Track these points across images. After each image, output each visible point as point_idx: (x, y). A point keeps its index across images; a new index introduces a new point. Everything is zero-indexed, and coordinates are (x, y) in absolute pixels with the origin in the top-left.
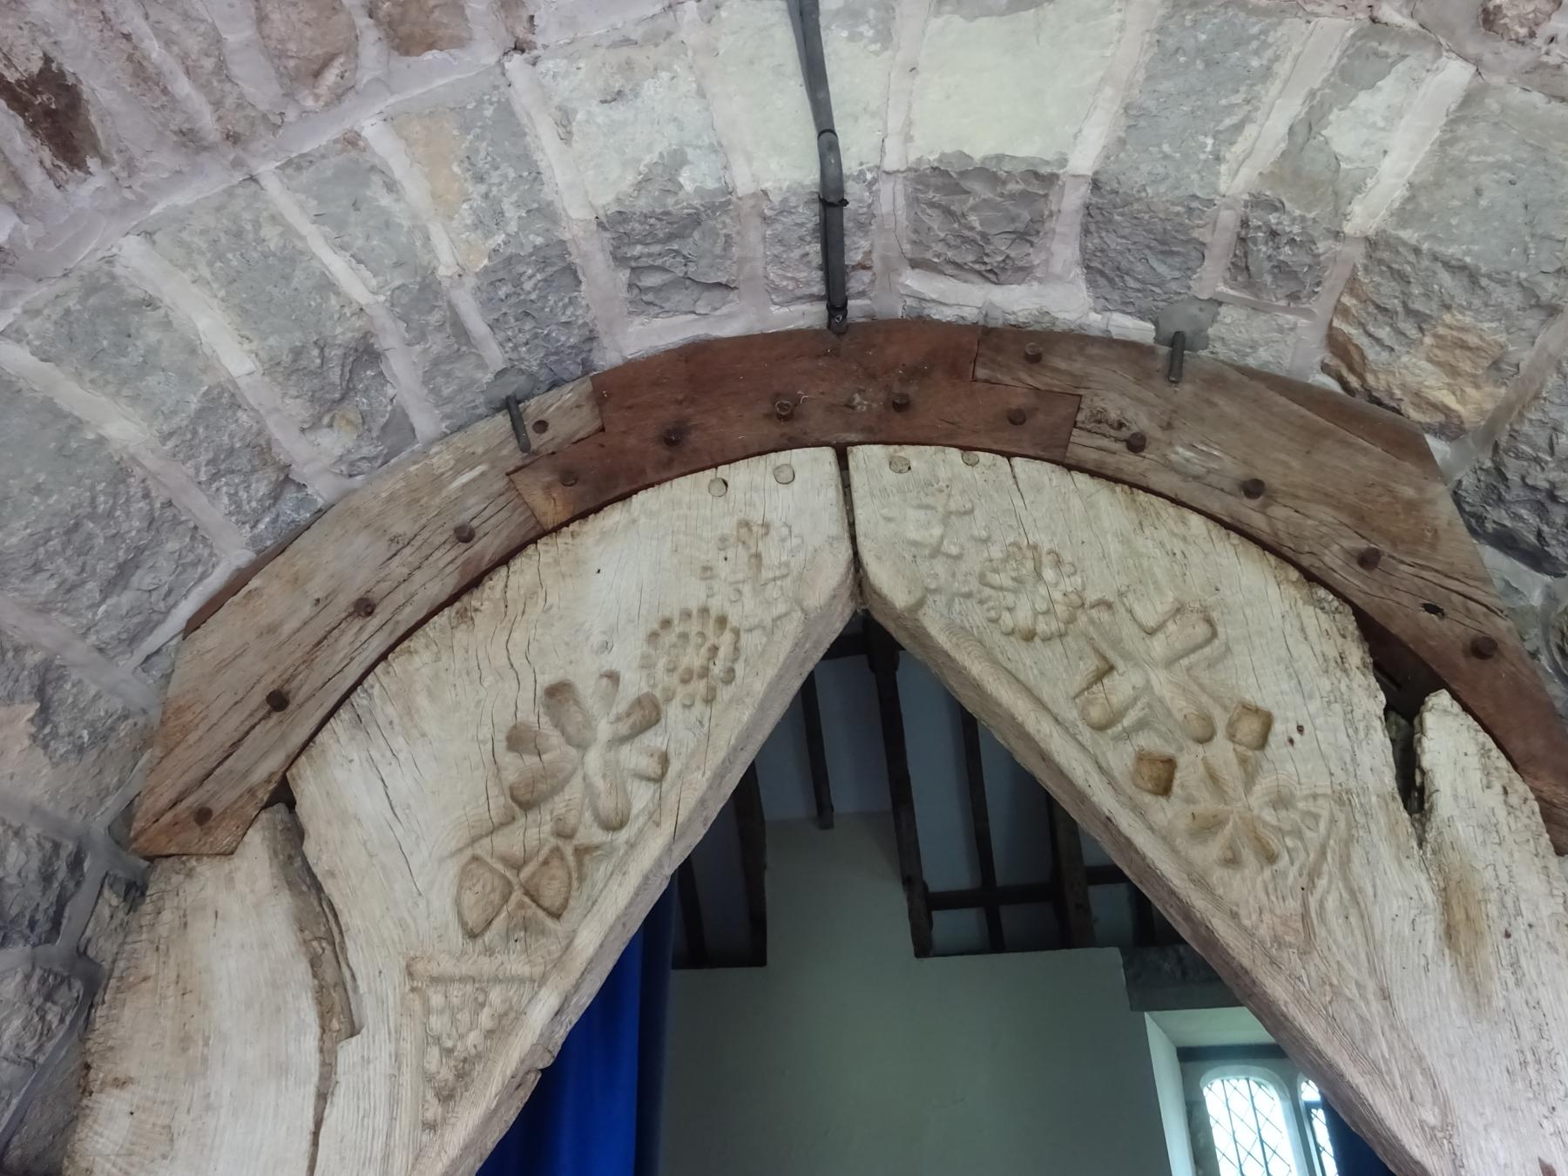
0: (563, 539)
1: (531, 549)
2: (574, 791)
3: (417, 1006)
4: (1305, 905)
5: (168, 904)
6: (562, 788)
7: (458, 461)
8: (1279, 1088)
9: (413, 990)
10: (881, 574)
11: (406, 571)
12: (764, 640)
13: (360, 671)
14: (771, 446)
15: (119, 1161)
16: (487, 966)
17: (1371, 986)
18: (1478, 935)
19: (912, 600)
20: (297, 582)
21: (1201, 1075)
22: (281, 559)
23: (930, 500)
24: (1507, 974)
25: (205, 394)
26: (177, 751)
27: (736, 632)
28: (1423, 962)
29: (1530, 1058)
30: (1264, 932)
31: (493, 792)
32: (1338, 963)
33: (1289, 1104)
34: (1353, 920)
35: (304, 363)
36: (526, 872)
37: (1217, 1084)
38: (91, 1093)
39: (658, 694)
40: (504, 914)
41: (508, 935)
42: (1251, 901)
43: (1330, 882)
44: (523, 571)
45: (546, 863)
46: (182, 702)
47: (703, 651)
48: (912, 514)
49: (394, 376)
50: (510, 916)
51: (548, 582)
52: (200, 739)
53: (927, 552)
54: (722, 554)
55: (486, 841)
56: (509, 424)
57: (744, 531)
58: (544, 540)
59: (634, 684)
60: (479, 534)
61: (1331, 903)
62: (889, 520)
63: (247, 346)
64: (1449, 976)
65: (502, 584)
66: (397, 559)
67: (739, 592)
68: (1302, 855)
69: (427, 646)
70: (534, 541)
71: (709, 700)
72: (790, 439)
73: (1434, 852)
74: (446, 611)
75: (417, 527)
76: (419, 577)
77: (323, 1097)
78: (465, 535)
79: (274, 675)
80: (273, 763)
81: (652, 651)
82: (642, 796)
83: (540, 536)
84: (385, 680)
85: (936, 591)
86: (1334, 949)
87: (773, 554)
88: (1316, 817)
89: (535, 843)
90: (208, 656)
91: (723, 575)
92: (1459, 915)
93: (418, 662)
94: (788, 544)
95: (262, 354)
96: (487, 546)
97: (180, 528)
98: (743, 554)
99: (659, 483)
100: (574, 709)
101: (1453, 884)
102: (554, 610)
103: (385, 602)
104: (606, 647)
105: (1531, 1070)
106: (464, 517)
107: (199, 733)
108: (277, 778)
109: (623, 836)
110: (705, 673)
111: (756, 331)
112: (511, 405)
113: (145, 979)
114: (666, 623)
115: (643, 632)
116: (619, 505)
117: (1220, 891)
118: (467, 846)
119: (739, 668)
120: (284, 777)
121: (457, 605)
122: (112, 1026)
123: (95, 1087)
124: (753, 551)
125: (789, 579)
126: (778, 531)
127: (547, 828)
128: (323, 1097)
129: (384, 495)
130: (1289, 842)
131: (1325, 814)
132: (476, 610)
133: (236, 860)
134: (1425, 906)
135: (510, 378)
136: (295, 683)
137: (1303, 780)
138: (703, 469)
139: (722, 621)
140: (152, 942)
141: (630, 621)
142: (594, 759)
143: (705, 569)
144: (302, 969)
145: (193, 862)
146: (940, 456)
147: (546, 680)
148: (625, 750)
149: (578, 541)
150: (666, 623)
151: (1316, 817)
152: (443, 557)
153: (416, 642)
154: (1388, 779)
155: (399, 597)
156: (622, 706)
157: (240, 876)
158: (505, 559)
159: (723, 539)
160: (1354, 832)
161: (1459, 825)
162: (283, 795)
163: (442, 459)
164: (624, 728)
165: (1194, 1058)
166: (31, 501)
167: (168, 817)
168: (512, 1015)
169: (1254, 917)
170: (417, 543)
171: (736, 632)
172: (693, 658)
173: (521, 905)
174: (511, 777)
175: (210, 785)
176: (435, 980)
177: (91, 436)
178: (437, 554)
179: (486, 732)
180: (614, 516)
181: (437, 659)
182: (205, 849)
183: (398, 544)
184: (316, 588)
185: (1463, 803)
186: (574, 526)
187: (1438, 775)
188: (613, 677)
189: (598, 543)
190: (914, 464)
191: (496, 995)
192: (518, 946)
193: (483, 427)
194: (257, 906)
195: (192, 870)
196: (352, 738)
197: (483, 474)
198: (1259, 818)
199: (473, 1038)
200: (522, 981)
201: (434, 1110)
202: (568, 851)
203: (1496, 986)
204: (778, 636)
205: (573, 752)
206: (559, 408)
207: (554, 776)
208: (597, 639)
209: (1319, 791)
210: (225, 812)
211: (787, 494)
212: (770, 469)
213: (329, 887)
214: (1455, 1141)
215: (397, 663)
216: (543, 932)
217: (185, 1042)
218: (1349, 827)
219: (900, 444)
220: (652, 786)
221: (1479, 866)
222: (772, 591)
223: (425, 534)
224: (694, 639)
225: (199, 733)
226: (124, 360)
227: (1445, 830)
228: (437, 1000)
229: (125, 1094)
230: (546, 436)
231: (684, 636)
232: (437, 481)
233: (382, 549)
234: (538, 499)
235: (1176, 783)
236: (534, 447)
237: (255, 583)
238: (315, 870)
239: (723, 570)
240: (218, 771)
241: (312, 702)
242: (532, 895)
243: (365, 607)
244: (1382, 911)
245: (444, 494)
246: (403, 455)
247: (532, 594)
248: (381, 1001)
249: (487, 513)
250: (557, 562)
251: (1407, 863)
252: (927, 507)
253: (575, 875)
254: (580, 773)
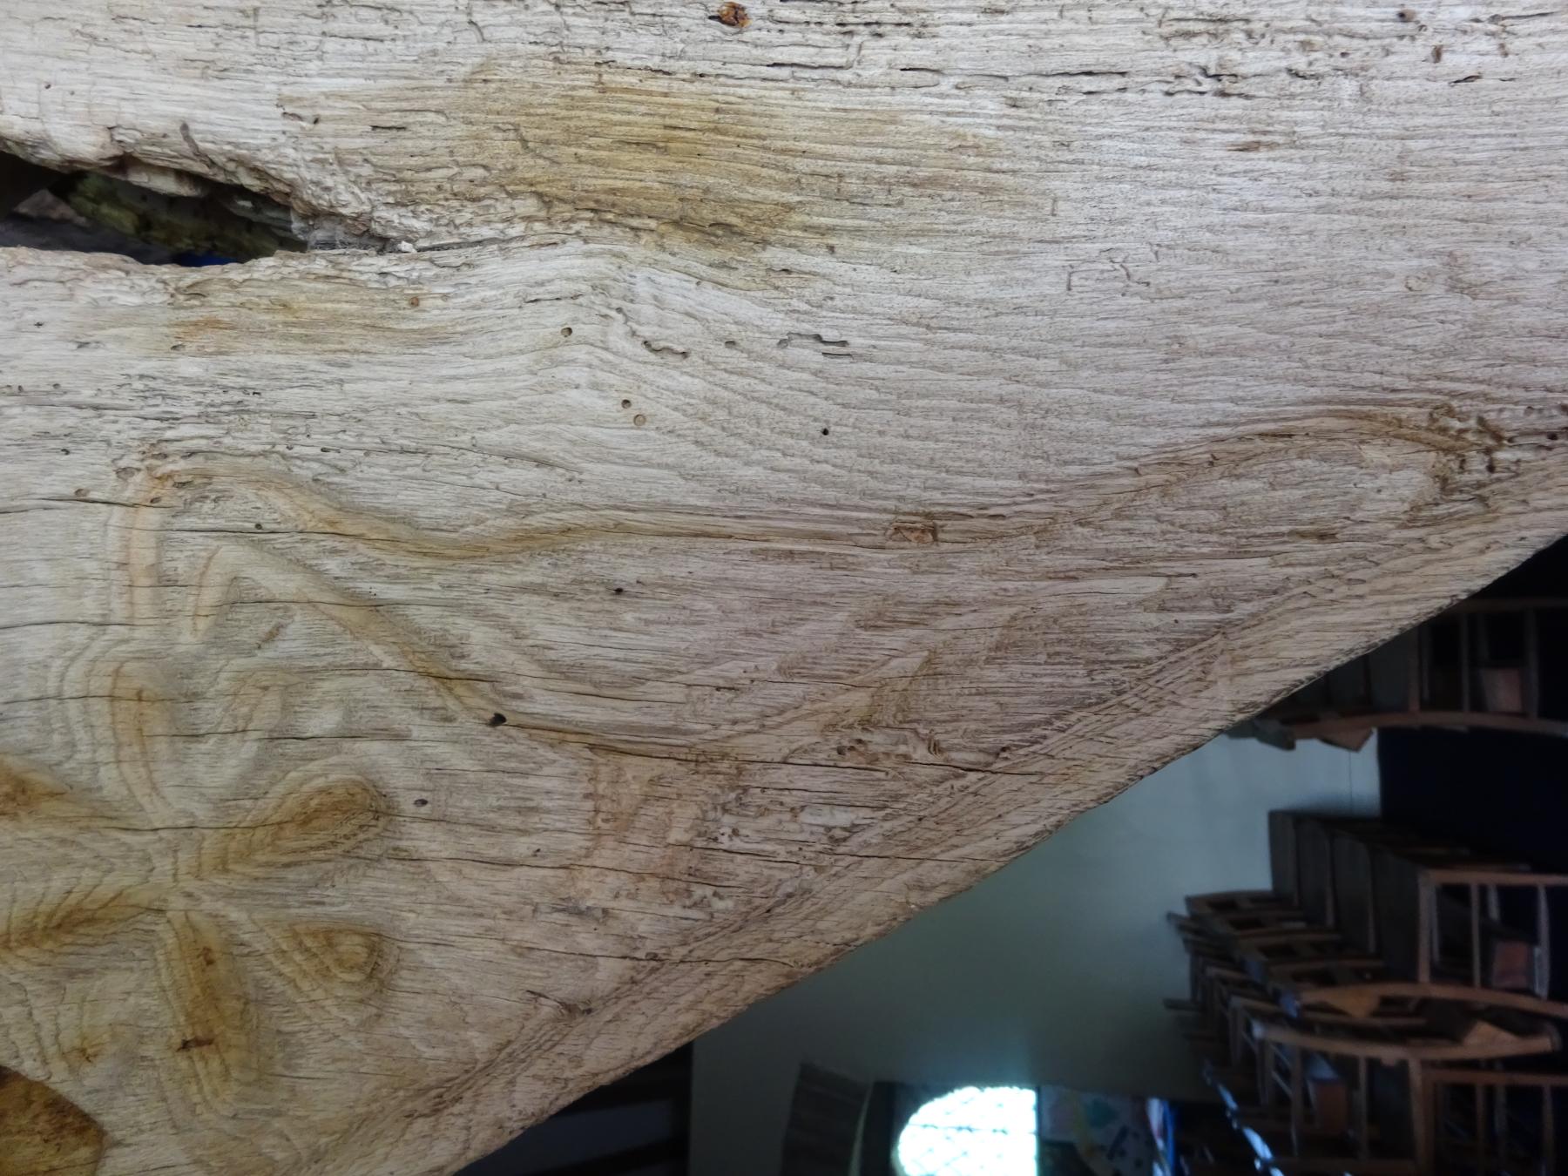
4: (557, 733)
17: (885, 572)
18: (725, 124)
24: (879, 56)
28: (811, 355)
29: (1201, 53)
30: (649, 918)
32: (788, 672)
34: (628, 572)
42: (526, 934)
43: (478, 613)
61: (561, 631)
64: (868, 274)
68: (369, 687)
73: (407, 201)
86: (733, 670)
88: (237, 598)
92: (644, 175)
101: (529, 167)
105: (1252, 61)
117: (480, 1043)
130: (324, 721)
131: (232, 555)
134: (600, 288)
137: (90, 607)
151: (237, 598)
154: (123, 291)
160: (305, 471)
161: (315, 84)
169: (587, 940)
185: (237, 50)
187: (129, 113)
198: (221, 804)
203: (923, 113)
209: (144, 555)
214: (1510, 419)
218: (284, 482)
221: (468, 53)
227: (333, 138)
235: (61, 1081)
244: (603, 454)
251: (433, 314)
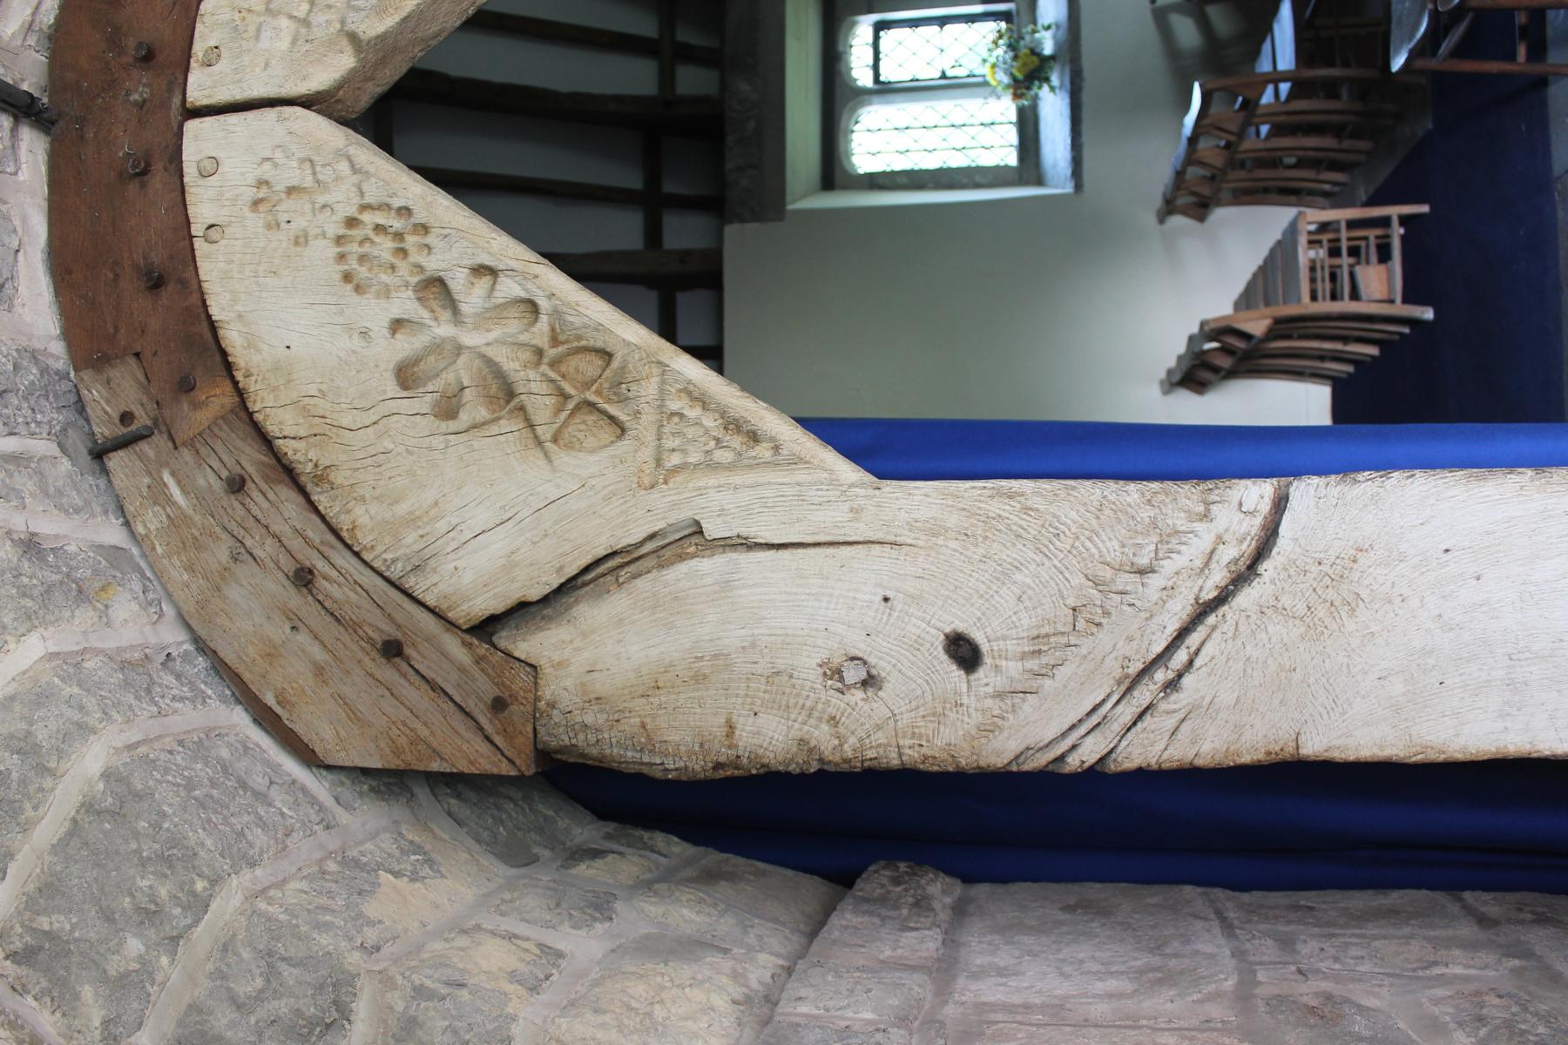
0: (251, 385)
1: (258, 417)
2: (501, 356)
3: (679, 478)
5: (578, 719)
6: (496, 364)
7: (155, 503)
8: (862, 104)
9: (666, 482)
10: (319, 79)
11: (269, 541)
12: (373, 180)
13: (368, 572)
14: (176, 179)
15: (793, 717)
16: (649, 416)
19: (349, 49)
20: (272, 654)
21: (847, 167)
22: (247, 676)
23: (252, 29)
25: (63, 679)
26: (435, 745)
27: (365, 208)
31: (494, 429)
33: (875, 98)
35: (36, 592)
36: (569, 389)
37: (856, 160)
38: (738, 757)
39: (416, 279)
40: (606, 406)
41: (623, 400)
44: (280, 421)
45: (564, 376)
46: (388, 751)
47: (377, 239)
48: (264, 43)
49: (57, 537)
50: (609, 401)
51: (294, 395)
52: (425, 724)
53: (303, 30)
54: (284, 226)
55: (539, 430)
56: (121, 453)
57: (262, 208)
58: (249, 405)
59: (405, 304)
60: (238, 469)
62: (267, 65)
63: (12, 646)
65: (292, 442)
66: (258, 552)
67: (324, 206)
69: (349, 512)
70: (250, 415)
71: (424, 229)
72: (170, 162)
74: (314, 498)
75: (224, 536)
76: (274, 528)
77: (748, 545)
78: (237, 485)
79: (366, 660)
80: (453, 645)
81: (374, 289)
82: (509, 288)
83: (247, 409)
84: (380, 549)
85: (343, 22)
87: (291, 174)
89: (544, 385)
90: (343, 734)
91: (304, 224)
93: (363, 519)
94: (280, 161)
95: (22, 630)
96: (250, 458)
97: (206, 743)
98: (288, 204)
99: (202, 294)
100: (422, 366)
102: (323, 387)
103: (300, 557)
104: (364, 334)
106: (217, 485)
107: (418, 726)
108: (467, 637)
109: (543, 303)
110: (399, 236)
111: (45, 204)
112: (99, 454)
113: (643, 726)
114: (347, 277)
115: (355, 298)
116: (221, 333)
118: (543, 448)
119: (397, 203)
120: (467, 631)
121: (309, 487)
122: (683, 748)
123: (732, 752)
124: (283, 196)
125: (315, 158)
126: (267, 171)
127: (532, 374)
128: (748, 545)
129: (186, 577)
132: (316, 466)
133: (543, 662)
135: (69, 443)
136: (375, 636)
138: (193, 250)
139: (352, 222)
140: (612, 727)
141: (342, 313)
142: (471, 339)
143: (297, 243)
144: (641, 584)
145: (542, 705)
146: (206, 19)
147: (392, 388)
148: (465, 308)
149: (254, 371)
150: (347, 277)
152: (258, 502)
153: (343, 523)
155: (295, 544)
156: (425, 314)
157: (556, 658)
158: (265, 440)
159: (269, 226)
162: (486, 627)
163: (151, 521)
164: (446, 315)
165: (833, 172)
166: (168, 830)
167: (498, 740)
168: (691, 388)
170: (240, 533)
171: (365, 208)
172: (385, 245)
173: (598, 393)
174: (483, 413)
175: (470, 705)
176: (659, 462)
177: (101, 786)
178: (255, 511)
179: (438, 442)
180: (233, 338)
181: (363, 499)
182: (531, 696)
183: (241, 553)
184: (279, 631)
186: (239, 376)
188: (397, 325)
189: (259, 351)
190: (213, 43)
191: (674, 406)
192: (634, 387)
193: (120, 480)
194: (584, 635)
195: (548, 704)
196: (434, 570)
197: (173, 474)
199: (710, 421)
200: (663, 382)
201: (763, 451)
202: (552, 353)
204: (372, 169)
205: (463, 359)
206: (108, 402)
207: (484, 378)
208: (357, 343)
210: (497, 684)
211: (225, 167)
212: (202, 182)
213: (571, 571)
215: (364, 539)
216: (623, 368)
217: (700, 678)
219: (190, 57)
220: (502, 278)
222: (325, 175)
223: (233, 526)
224: (367, 248)
225: (418, 726)
226: (15, 775)
228: (675, 459)
229: (740, 722)
230: (138, 411)
231: (363, 259)
232: (177, 522)
233: (246, 570)
234: (203, 417)
236: (149, 423)
237: (270, 699)
238: (555, 585)
239: (300, 223)
240: (458, 699)
241: (395, 615)
242: (587, 385)
243: (304, 578)
245: (190, 512)
246: (143, 564)
247: (306, 412)
248: (674, 506)
249: (216, 464)
250: (276, 389)
252: (258, 31)
253: (575, 344)
254: (484, 350)
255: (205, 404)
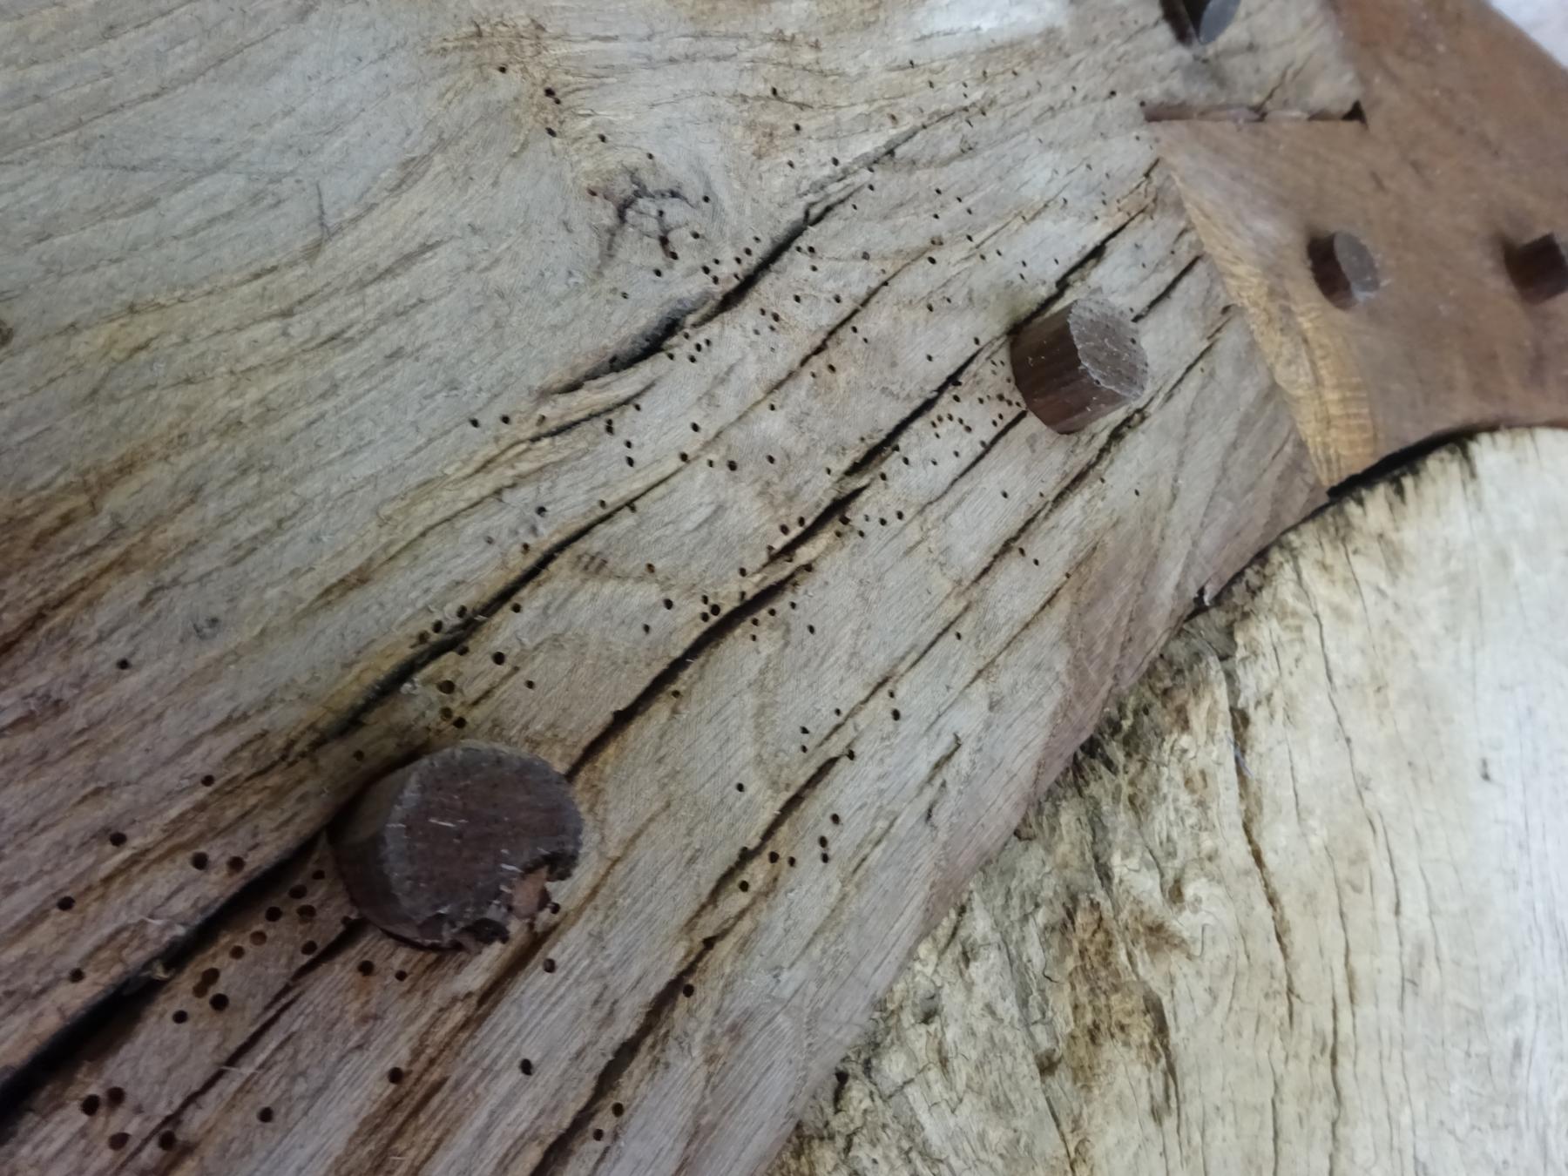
11: (755, 522)
66: (670, 405)
170: (806, 293)
178: (932, 453)
255: (1285, 320)
